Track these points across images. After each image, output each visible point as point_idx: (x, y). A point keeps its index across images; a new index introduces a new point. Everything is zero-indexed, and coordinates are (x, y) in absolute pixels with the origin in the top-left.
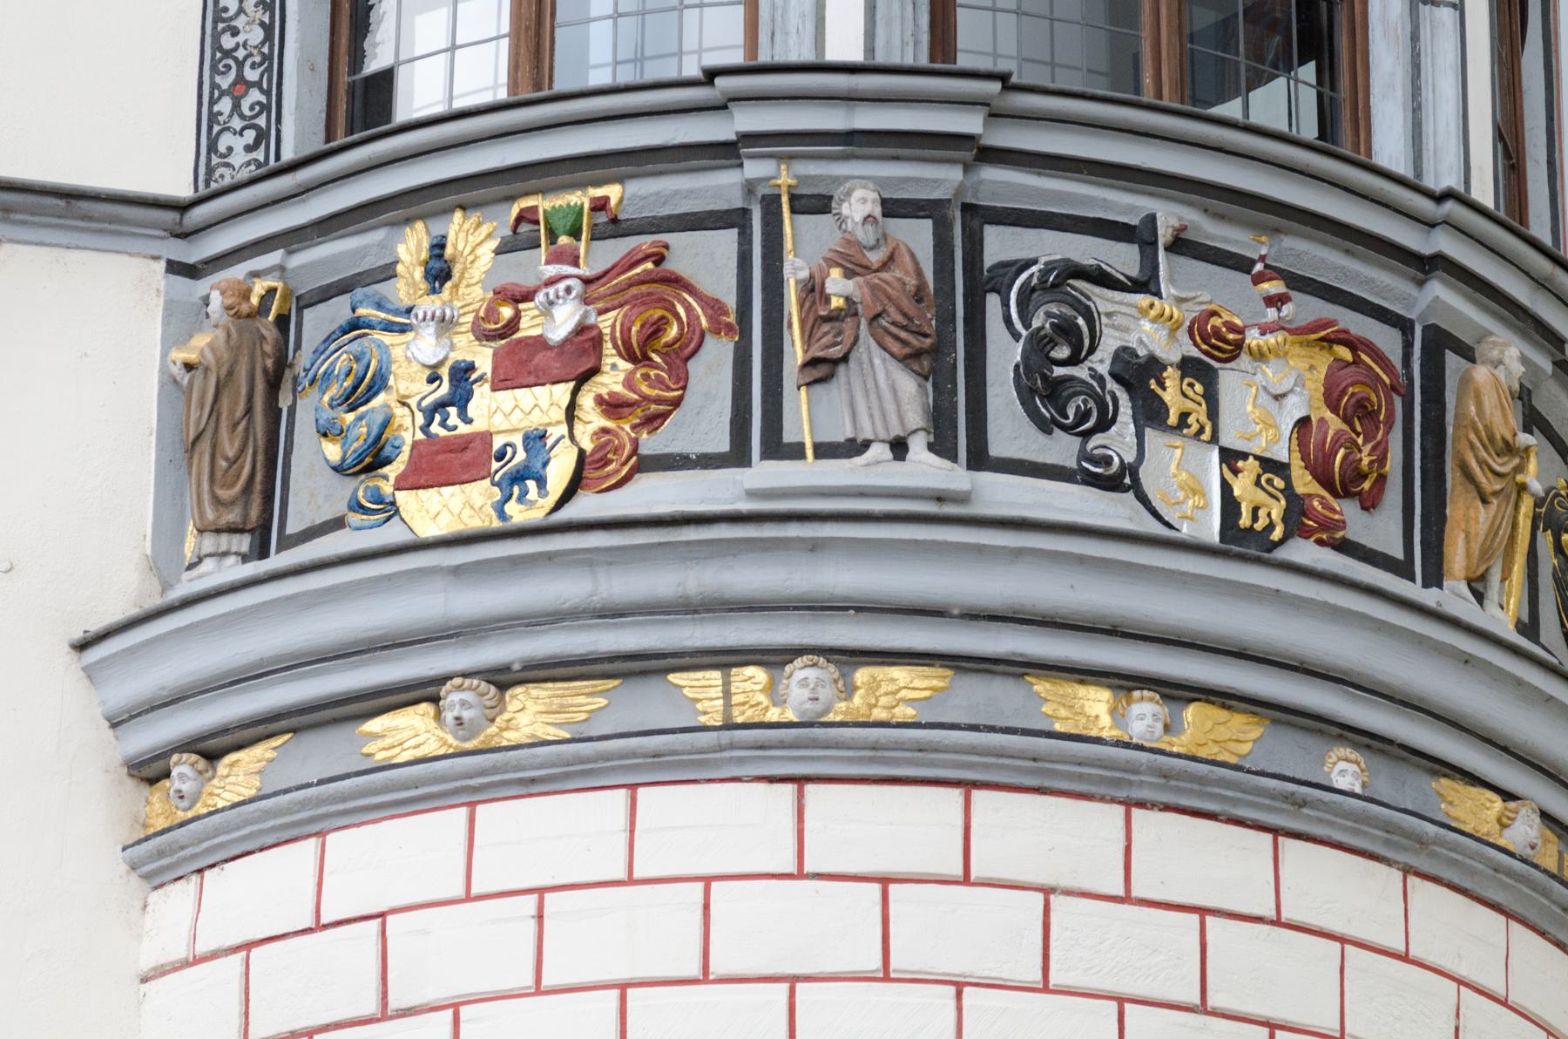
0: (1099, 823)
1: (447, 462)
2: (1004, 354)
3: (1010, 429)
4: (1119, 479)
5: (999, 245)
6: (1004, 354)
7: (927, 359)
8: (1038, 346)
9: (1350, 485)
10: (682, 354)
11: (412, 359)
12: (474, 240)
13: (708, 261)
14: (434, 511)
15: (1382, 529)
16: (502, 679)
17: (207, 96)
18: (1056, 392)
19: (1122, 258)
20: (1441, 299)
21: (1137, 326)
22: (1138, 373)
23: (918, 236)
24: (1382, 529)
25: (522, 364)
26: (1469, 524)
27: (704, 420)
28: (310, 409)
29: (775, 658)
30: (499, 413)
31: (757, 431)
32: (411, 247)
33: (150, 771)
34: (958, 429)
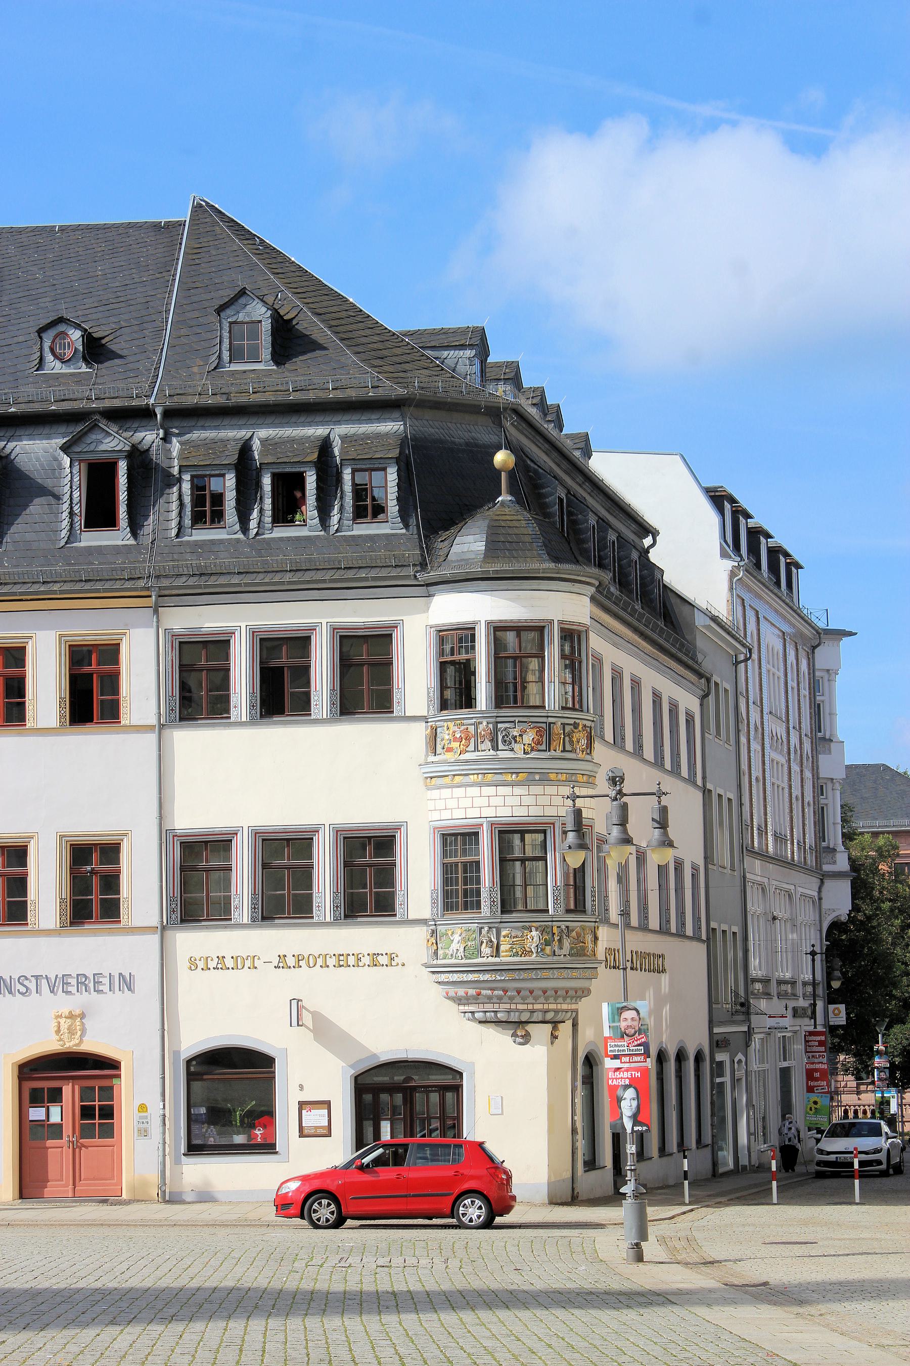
0: (510, 788)
1: (450, 750)
2: (500, 738)
3: (501, 746)
4: (512, 750)
5: (499, 725)
6: (500, 738)
7: (492, 741)
8: (503, 737)
9: (539, 743)
10: (469, 740)
11: (447, 737)
12: (451, 724)
13: (472, 729)
14: (449, 756)
15: (543, 747)
16: (454, 775)
17: (428, 701)
18: (505, 741)
19: (511, 725)
20: (551, 720)
21: (516, 733)
22: (514, 738)
23: (491, 726)
24: (543, 747)
25: (455, 740)
26: (554, 744)
27: (471, 747)
28: (438, 740)
29: (478, 774)
30: (455, 745)
31: (476, 749)
32: (445, 724)
33: (427, 778)
34: (495, 748)
